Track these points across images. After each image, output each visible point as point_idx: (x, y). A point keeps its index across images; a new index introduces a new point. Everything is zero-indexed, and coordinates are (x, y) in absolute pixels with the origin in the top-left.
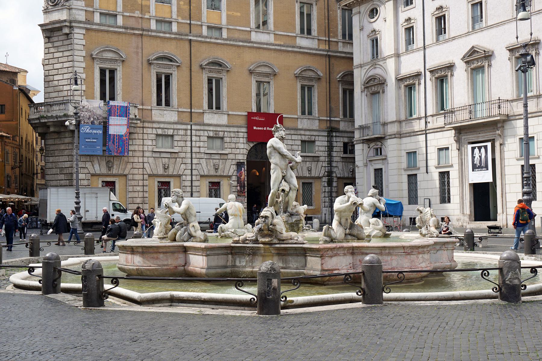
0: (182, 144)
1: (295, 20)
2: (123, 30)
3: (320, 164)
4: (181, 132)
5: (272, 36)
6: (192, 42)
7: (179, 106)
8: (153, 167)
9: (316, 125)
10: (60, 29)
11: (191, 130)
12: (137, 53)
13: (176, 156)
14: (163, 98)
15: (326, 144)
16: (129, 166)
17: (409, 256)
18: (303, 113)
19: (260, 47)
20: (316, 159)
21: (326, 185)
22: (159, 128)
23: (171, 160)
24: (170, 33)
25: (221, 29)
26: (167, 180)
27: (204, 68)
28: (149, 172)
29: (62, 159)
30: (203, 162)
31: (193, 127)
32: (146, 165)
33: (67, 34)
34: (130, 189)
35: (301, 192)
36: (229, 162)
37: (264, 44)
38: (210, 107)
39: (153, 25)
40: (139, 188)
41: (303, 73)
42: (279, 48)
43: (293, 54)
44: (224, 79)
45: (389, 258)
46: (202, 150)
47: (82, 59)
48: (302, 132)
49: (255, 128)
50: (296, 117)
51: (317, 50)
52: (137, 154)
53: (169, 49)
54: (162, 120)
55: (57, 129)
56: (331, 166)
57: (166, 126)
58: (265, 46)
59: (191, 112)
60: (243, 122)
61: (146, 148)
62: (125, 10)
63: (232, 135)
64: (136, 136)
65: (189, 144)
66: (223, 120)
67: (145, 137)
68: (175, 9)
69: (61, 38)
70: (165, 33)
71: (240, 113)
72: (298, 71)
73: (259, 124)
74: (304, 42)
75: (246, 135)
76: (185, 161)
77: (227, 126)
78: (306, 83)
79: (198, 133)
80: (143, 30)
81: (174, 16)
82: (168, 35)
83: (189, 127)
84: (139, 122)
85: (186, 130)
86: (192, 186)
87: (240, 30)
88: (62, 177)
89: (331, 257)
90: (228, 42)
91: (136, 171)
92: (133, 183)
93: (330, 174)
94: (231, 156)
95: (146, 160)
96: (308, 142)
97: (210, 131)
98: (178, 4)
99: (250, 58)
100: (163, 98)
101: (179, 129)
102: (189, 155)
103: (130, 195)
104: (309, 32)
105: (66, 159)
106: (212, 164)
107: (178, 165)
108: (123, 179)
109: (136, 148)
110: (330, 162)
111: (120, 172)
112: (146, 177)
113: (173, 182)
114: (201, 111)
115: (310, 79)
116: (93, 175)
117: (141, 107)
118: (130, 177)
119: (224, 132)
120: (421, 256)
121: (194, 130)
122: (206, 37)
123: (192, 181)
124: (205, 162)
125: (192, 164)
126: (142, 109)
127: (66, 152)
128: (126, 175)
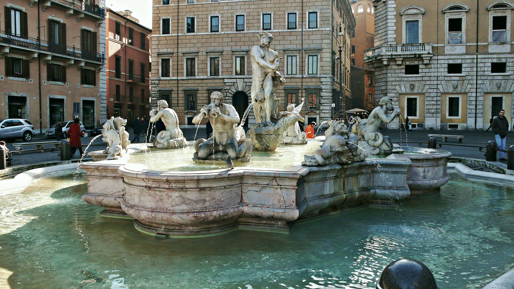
0: (469, 69)
7: (467, 42)
8: (445, 87)
11: (477, 58)
13: (464, 78)
16: (427, 87)
22: (450, 59)
23: (459, 82)
26: (456, 96)
27: (490, 10)
28: (442, 91)
29: (382, 84)
30: (487, 83)
31: (479, 56)
32: (440, 87)
34: (427, 103)
40: (433, 102)
46: (486, 73)
47: (393, 17)
52: (432, 78)
55: (378, 65)
57: (456, 57)
59: (477, 45)
61: (439, 74)
64: (433, 66)
65: (475, 69)
76: (471, 82)
77: (509, 53)
79: (483, 61)
83: (475, 56)
84: (432, 56)
85: (474, 59)
86: (476, 101)
91: (432, 91)
92: (429, 99)
95: (439, 82)
97: (494, 58)
101: (467, 59)
102: (475, 78)
103: (426, 107)
106: (495, 84)
107: (465, 85)
108: (422, 96)
109: (432, 74)
111: (420, 91)
113: (460, 97)
114: (486, 44)
116: (400, 94)
117: (436, 45)
118: (427, 95)
119: (507, 58)
121: (480, 58)
123: (476, 97)
124: (488, 82)
125: (477, 84)
126: (437, 47)
128: (424, 94)
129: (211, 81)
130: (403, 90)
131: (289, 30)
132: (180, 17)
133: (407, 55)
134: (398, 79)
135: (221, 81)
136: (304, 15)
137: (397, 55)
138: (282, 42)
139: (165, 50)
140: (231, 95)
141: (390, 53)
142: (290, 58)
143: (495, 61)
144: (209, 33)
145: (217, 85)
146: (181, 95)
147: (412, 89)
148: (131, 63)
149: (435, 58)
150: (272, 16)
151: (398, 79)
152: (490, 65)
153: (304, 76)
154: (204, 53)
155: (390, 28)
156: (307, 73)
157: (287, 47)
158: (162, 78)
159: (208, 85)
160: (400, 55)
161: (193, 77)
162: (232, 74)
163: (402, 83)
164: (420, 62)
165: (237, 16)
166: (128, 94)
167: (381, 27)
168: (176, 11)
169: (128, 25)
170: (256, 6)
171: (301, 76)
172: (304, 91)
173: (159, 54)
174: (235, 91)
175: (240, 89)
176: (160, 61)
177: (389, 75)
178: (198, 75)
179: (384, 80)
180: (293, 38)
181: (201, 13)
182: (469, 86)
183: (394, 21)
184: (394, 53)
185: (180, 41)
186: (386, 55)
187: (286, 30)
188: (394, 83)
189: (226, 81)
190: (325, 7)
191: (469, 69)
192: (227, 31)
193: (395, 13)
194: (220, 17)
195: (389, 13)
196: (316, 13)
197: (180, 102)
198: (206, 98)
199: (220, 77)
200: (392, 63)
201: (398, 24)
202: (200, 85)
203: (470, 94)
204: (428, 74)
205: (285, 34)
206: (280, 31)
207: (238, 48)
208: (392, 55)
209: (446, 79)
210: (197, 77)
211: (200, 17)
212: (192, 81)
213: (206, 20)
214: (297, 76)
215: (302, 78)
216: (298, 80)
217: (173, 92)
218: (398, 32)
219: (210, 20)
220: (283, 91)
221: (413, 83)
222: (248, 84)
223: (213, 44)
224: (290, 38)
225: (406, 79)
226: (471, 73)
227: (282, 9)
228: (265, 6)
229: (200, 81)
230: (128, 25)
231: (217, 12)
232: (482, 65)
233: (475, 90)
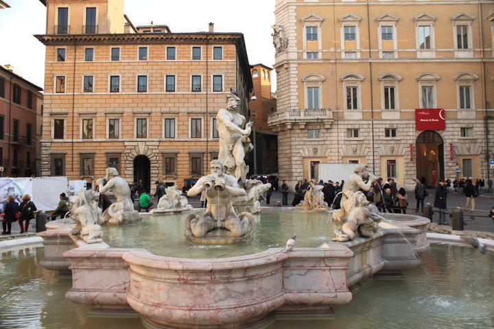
0: (366, 134)
1: (453, 39)
2: (322, 61)
3: (478, 145)
4: (364, 126)
5: (434, 52)
6: (373, 65)
9: (473, 115)
10: (283, 65)
11: (373, 124)
12: (333, 75)
14: (352, 103)
15: (483, 129)
16: (328, 151)
17: (188, 287)
18: (462, 107)
19: (424, 62)
20: (474, 141)
21: (483, 160)
24: (355, 60)
25: (392, 52)
31: (374, 122)
33: (287, 68)
35: (462, 166)
36: (401, 146)
37: (428, 59)
38: (387, 107)
39: (343, 56)
41: (461, 77)
42: (440, 61)
43: (452, 64)
44: (397, 87)
45: (155, 285)
46: (381, 138)
47: (295, 83)
48: (462, 121)
49: (421, 120)
50: (456, 110)
51: (472, 59)
52: (334, 142)
53: (354, 70)
54: (352, 118)
56: (488, 146)
57: (355, 122)
58: (428, 61)
60: (413, 116)
61: (340, 138)
62: (323, 48)
63: (404, 126)
64: (332, 130)
66: (396, 115)
67: (339, 130)
68: (358, 43)
69: (284, 72)
70: (351, 60)
71: (410, 110)
72: (457, 76)
73: (424, 117)
74: (462, 54)
75: (415, 126)
76: (368, 146)
78: (464, 84)
79: (377, 126)
80: (336, 60)
81: (358, 48)
82: (354, 61)
86: (374, 163)
87: (408, 52)
88: (286, 159)
89: (91, 270)
90: (399, 61)
91: (333, 154)
93: (487, 151)
94: (402, 142)
95: (340, 146)
96: (467, 128)
98: (361, 40)
99: (416, 71)
100: (352, 103)
102: (371, 142)
104: (466, 47)
105: (288, 147)
109: (333, 138)
110: (487, 143)
112: (340, 158)
115: (467, 81)
120: (221, 286)
122: (382, 59)
127: (288, 144)
129: (110, 144)
130: (307, 154)
131: (194, 93)
132: (76, 76)
133: (310, 120)
134: (301, 143)
135: (121, 144)
136: (209, 78)
137: (301, 120)
138: (185, 105)
139: (59, 110)
140: (131, 159)
141: (293, 118)
142: (194, 121)
143: (387, 126)
144: (109, 93)
145: (117, 148)
146: (76, 159)
147: (315, 153)
148: (16, 123)
149: (336, 123)
150: (176, 78)
151: (301, 143)
152: (384, 130)
153: (209, 140)
154: (103, 115)
155: (293, 94)
156: (212, 137)
157: (191, 110)
158: (55, 140)
159: (107, 148)
160: (304, 120)
161: (89, 140)
162: (133, 137)
163: (305, 147)
164: (322, 127)
165: (139, 76)
166: (12, 158)
167: (284, 93)
168: (73, 68)
169: (14, 81)
170: (159, 67)
171: (206, 139)
172: (209, 155)
173: (51, 114)
174: (136, 155)
175: (142, 153)
176: (53, 122)
177: (293, 139)
178: (95, 138)
179: (288, 144)
180: (198, 100)
181: (100, 72)
182: (367, 150)
183: (297, 87)
184: (297, 118)
185: (76, 101)
186: (290, 120)
187: (190, 93)
188: (298, 147)
189: (126, 144)
190: (229, 71)
191: (366, 134)
192: (129, 91)
193: (297, 79)
194: (120, 77)
195: (292, 80)
196: (221, 76)
197: (75, 166)
198: (104, 162)
199: (120, 139)
200: (295, 127)
201: (300, 89)
202: (98, 148)
203: (367, 157)
204: (330, 138)
205: (189, 97)
206: (184, 93)
207: (140, 110)
208: (295, 120)
209: (346, 143)
210: (94, 140)
211: (99, 76)
212: (89, 144)
213: (105, 79)
214: (202, 139)
215: (208, 141)
216: (203, 144)
217: (67, 156)
218: (300, 97)
219: (109, 79)
220: (188, 155)
221: (316, 147)
222: (150, 147)
223: (112, 105)
224: (193, 101)
225: (309, 143)
226: (368, 138)
227: (186, 71)
228: (168, 67)
229: (98, 144)
230: (14, 81)
231: (118, 72)
232: (377, 130)
233: (372, 154)
